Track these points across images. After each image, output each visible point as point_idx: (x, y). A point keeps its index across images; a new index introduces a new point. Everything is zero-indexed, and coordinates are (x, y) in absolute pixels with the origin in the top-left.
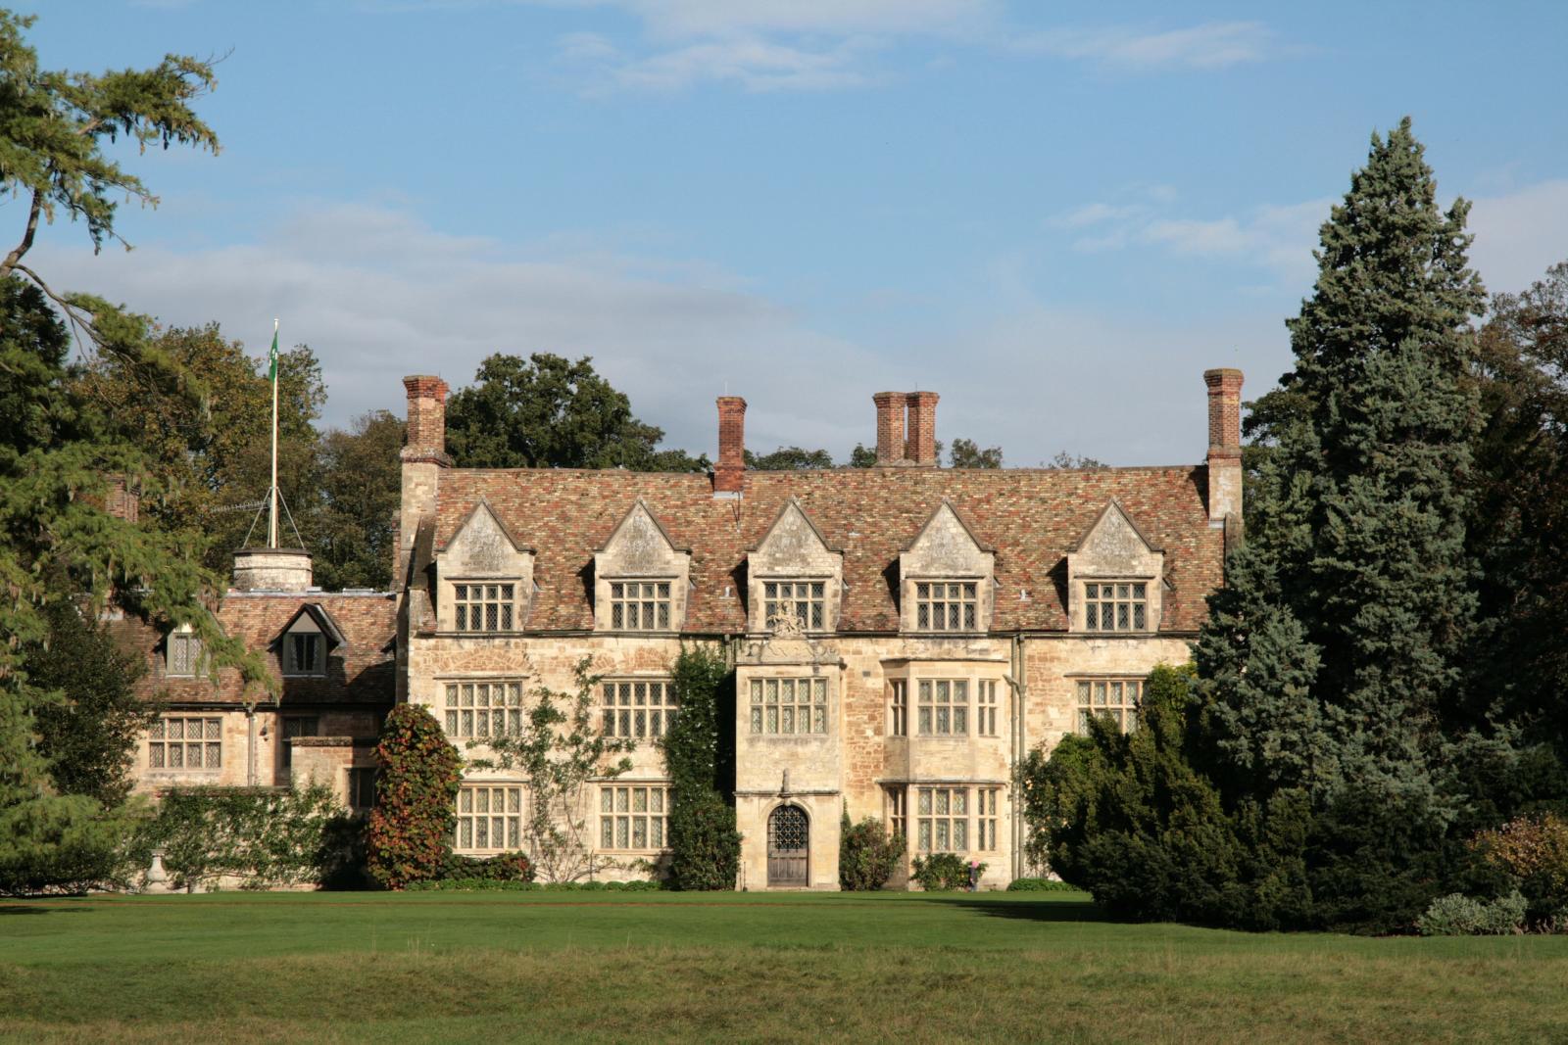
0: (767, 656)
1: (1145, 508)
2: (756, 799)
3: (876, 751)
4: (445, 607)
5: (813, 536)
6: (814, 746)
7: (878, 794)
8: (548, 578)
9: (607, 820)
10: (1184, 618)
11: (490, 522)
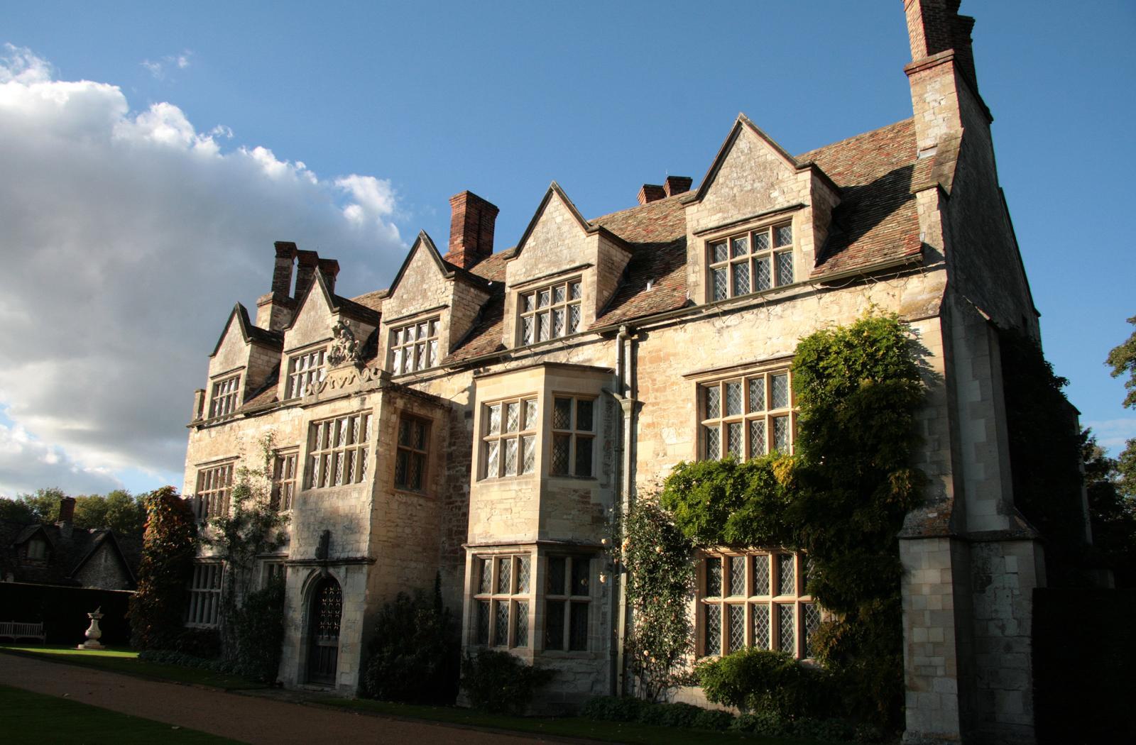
1: (840, 169)
2: (301, 568)
10: (852, 257)
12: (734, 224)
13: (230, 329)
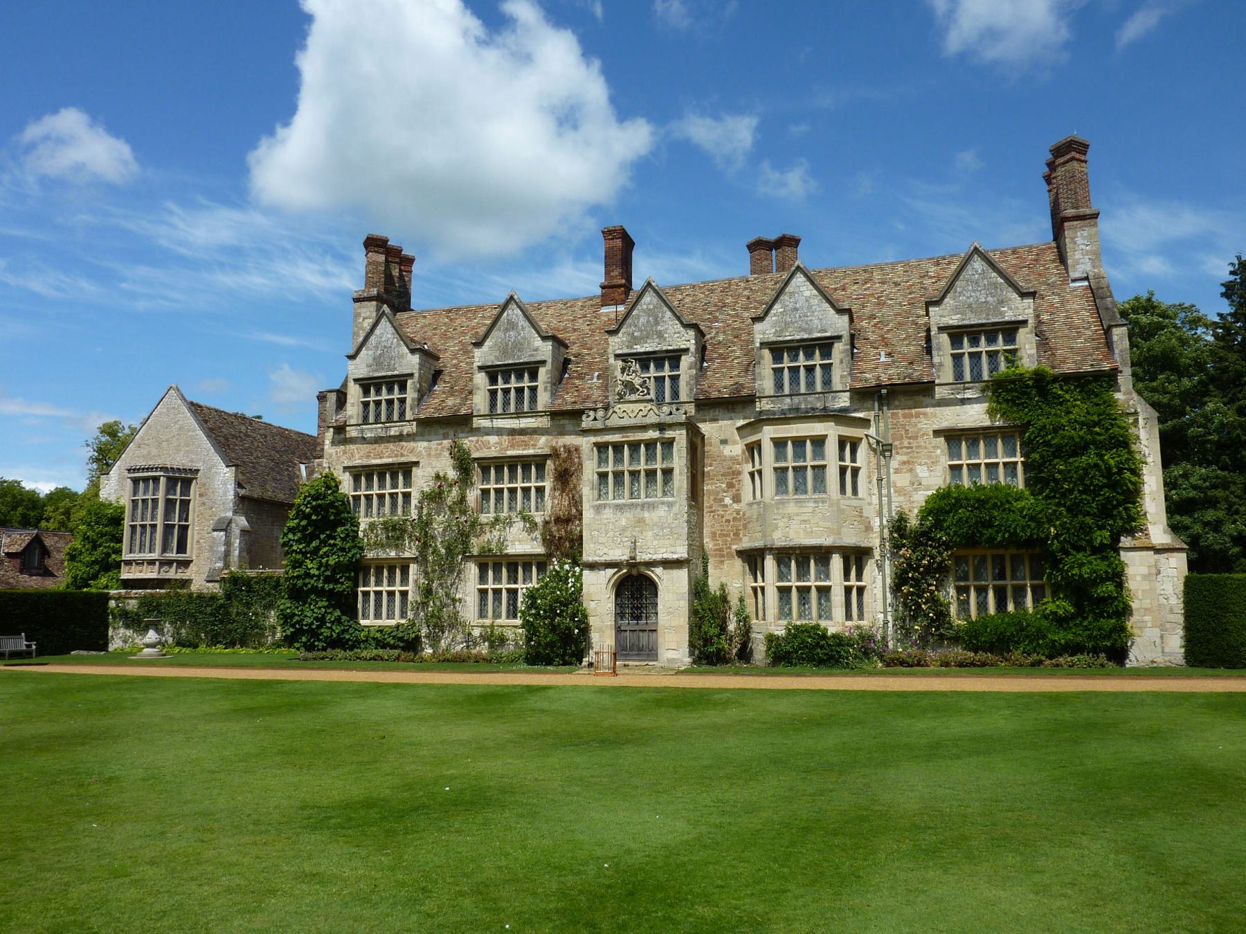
0: (614, 421)
3: (735, 519)
4: (353, 405)
5: (668, 314)
6: (662, 511)
7: (738, 563)
8: (447, 379)
9: (483, 593)
11: (390, 329)
12: (972, 326)
13: (378, 331)
